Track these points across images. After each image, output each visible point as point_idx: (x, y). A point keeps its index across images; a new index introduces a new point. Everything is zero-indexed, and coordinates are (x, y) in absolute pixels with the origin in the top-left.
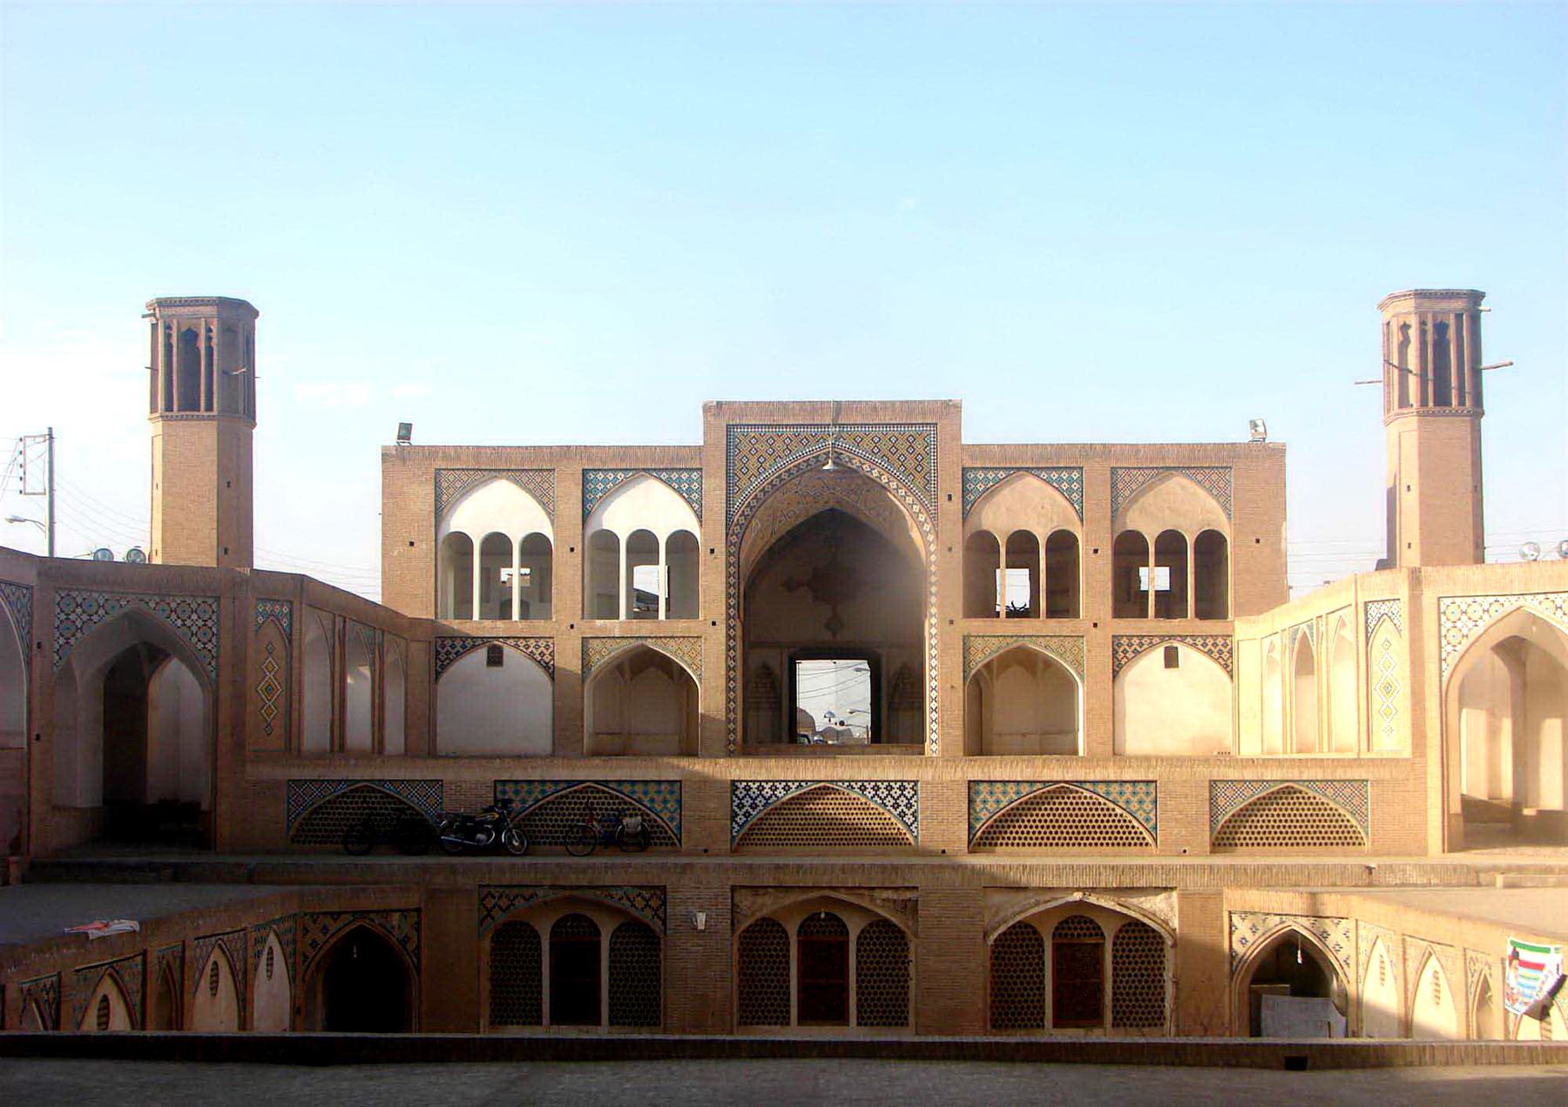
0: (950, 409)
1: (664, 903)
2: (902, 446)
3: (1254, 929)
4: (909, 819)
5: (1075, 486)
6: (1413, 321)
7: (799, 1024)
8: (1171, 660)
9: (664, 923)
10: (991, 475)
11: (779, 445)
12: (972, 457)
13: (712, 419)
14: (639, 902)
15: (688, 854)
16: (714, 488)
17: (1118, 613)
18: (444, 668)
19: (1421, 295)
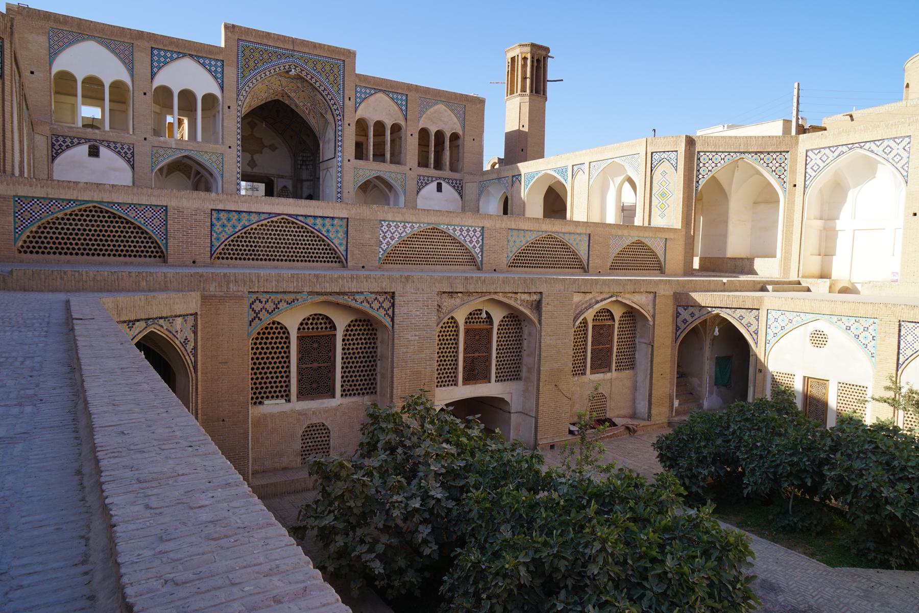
0: (350, 55)
1: (393, 305)
2: (327, 68)
3: (692, 315)
4: (478, 250)
5: (404, 103)
6: (529, 56)
7: (464, 384)
8: (439, 188)
9: (393, 320)
10: (368, 91)
11: (265, 56)
12: (360, 80)
13: (229, 34)
14: (376, 305)
15: (355, 268)
16: (231, 73)
17: (420, 165)
18: (58, 154)
19: (533, 46)
